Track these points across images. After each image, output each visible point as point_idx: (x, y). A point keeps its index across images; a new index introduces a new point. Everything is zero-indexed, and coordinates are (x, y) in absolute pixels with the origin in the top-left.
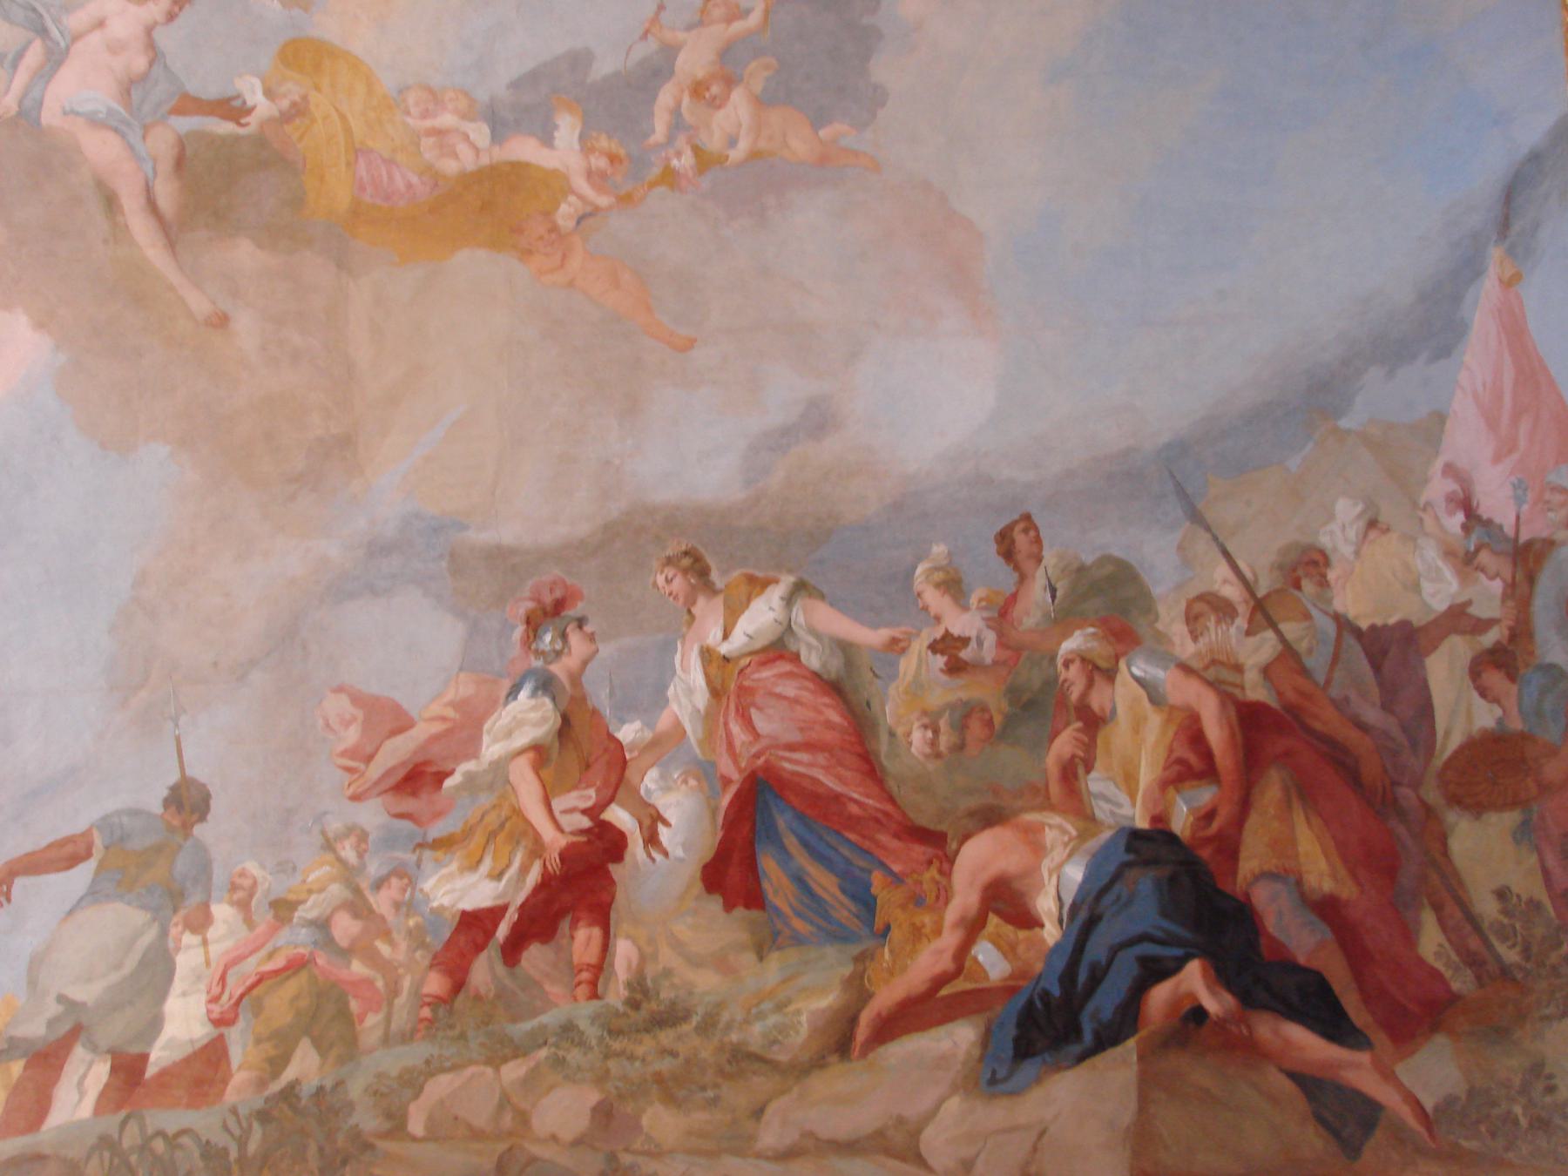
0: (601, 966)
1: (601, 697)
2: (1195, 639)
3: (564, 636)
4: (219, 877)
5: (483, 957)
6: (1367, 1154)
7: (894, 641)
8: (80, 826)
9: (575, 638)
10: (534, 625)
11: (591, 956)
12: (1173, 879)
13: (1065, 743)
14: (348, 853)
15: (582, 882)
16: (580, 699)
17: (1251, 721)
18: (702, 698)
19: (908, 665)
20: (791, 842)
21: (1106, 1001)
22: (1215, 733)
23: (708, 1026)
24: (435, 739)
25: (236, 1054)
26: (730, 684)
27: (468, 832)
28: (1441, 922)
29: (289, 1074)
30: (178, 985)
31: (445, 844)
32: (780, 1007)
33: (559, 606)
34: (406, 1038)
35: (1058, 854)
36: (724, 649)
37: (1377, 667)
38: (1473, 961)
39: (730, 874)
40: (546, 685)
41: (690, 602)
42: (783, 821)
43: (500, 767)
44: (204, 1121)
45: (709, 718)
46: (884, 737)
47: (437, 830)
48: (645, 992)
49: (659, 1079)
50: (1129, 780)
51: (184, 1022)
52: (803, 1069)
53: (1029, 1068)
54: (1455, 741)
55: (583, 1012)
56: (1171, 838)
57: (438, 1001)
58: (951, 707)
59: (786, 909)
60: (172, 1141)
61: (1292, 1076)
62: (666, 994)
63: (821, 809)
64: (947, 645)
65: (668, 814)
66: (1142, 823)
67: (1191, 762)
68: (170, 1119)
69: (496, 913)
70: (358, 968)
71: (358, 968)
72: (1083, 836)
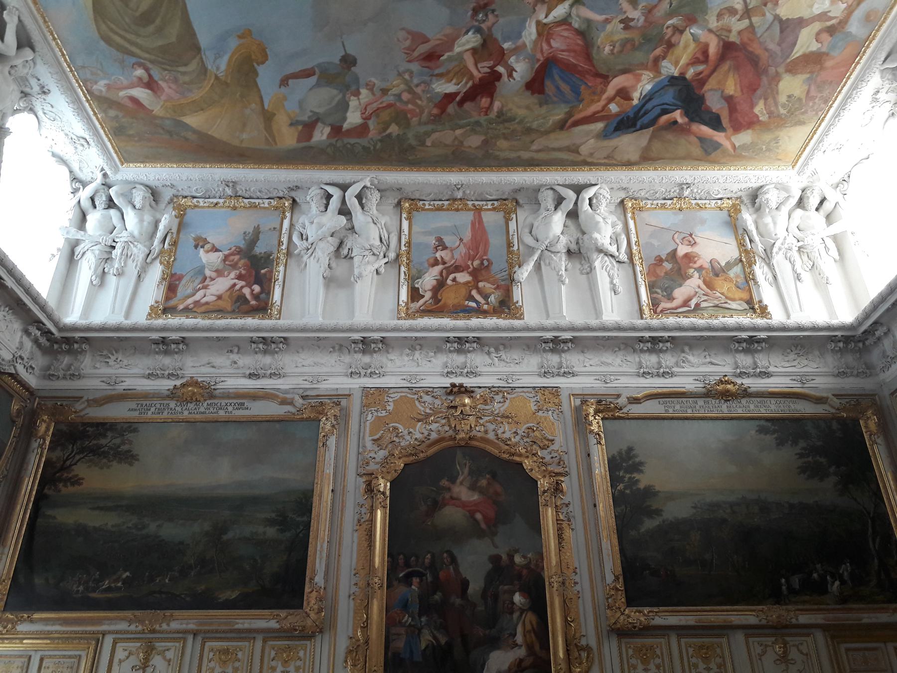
1: (498, 36)
2: (718, 20)
3: (487, 15)
4: (362, 82)
5: (451, 106)
6: (713, 155)
7: (607, 19)
9: (490, 16)
10: (476, 11)
11: (487, 105)
12: (680, 90)
13: (658, 51)
14: (407, 76)
16: (490, 35)
17: (728, 48)
18: (534, 36)
19: (609, 27)
20: (557, 77)
22: (713, 50)
23: (519, 123)
24: (438, 45)
25: (371, 127)
26: (545, 31)
27: (448, 72)
28: (765, 104)
29: (388, 131)
30: (351, 109)
31: (441, 75)
32: (544, 118)
33: (486, 5)
34: (425, 124)
35: (645, 82)
36: (545, 21)
37: (782, 31)
38: (770, 114)
39: (535, 85)
40: (478, 30)
41: (535, 5)
42: (555, 72)
43: (460, 54)
44: (364, 142)
45: (535, 42)
46: (596, 48)
47: (437, 72)
48: (503, 114)
49: (504, 134)
50: (676, 63)
51: (353, 118)
52: (547, 133)
53: (618, 133)
54: (797, 55)
55: (483, 119)
56: (685, 79)
57: (435, 116)
58: (622, 40)
59: (551, 94)
60: (353, 145)
61: (697, 137)
62: (509, 114)
63: (569, 69)
64: (626, 23)
65: (517, 69)
66: (676, 74)
67: (702, 55)
68: (352, 141)
69: (456, 94)
70: (410, 106)
71: (410, 106)
72: (654, 78)
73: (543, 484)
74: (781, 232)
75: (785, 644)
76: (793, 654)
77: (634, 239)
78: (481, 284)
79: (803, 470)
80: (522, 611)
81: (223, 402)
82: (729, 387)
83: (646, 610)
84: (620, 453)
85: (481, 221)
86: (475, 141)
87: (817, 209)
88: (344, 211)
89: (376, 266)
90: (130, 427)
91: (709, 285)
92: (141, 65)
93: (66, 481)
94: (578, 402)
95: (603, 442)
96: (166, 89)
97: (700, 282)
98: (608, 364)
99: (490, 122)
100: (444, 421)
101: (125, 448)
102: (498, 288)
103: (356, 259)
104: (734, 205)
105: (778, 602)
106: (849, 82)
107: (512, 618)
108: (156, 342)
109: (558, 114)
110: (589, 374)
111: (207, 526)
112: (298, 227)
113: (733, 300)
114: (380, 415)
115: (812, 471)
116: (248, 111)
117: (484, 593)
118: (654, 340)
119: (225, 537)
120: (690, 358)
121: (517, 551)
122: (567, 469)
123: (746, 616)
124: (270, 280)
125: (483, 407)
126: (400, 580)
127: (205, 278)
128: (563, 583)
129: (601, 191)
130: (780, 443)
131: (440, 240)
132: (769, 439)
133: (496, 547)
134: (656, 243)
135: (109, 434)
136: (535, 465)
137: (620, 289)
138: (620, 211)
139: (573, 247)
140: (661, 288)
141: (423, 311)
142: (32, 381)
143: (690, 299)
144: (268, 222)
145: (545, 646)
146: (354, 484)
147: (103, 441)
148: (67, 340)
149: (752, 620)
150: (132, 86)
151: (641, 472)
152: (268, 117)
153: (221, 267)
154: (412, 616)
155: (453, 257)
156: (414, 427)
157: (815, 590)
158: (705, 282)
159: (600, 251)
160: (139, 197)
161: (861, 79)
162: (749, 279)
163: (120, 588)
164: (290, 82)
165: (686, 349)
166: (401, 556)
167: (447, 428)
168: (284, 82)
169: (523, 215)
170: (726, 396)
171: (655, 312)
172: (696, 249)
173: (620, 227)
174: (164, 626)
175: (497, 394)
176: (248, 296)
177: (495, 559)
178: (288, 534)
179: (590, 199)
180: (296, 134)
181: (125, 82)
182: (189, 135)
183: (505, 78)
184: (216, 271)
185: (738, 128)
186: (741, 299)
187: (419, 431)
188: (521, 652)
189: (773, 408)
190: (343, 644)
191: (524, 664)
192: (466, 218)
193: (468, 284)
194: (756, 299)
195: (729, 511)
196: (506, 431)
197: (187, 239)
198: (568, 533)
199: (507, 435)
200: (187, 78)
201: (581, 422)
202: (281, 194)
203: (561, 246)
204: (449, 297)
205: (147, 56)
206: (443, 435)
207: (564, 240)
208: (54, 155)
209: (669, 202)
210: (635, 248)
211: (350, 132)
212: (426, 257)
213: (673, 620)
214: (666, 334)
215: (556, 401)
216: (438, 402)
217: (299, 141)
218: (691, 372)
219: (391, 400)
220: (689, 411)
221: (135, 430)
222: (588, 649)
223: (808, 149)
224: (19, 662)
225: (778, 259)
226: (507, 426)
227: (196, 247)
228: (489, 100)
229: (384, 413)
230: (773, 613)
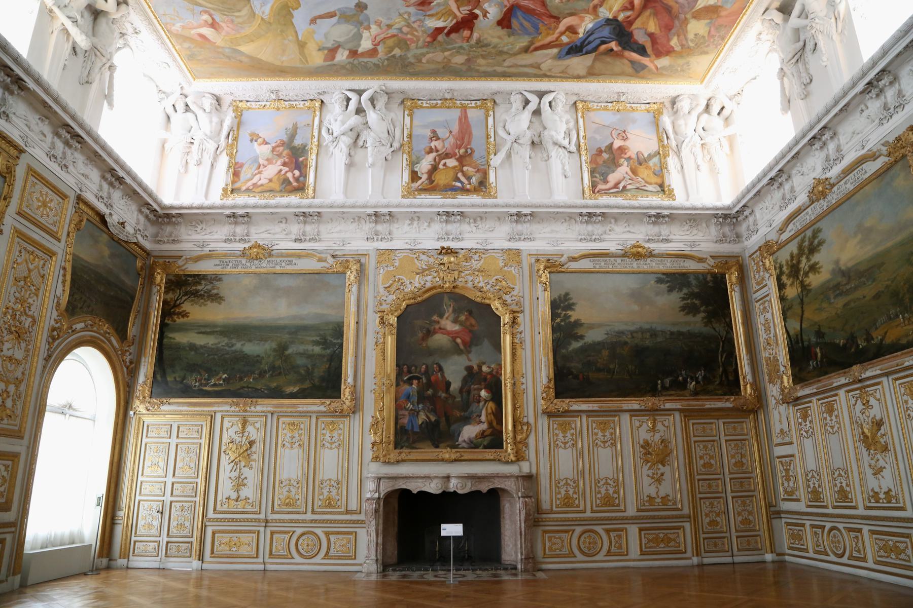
0: (468, 39)
4: (372, 20)
6: (641, 73)
8: (332, 10)
14: (406, 16)
15: (468, 23)
20: (521, 18)
21: (590, 47)
27: (437, 14)
31: (432, 15)
38: (682, 46)
39: (505, 22)
42: (519, 13)
44: (374, 60)
47: (428, 13)
50: (610, 10)
51: (366, 44)
52: (515, 54)
55: (465, 45)
56: (617, 20)
57: (429, 42)
62: (485, 42)
63: (528, 11)
66: (611, 17)
68: (366, 60)
69: (444, 28)
70: (409, 36)
73: (506, 318)
74: (690, 132)
75: (655, 420)
76: (659, 426)
77: (582, 134)
78: (465, 168)
79: (683, 309)
80: (486, 401)
81: (279, 259)
82: (640, 250)
83: (568, 400)
84: (560, 297)
85: (466, 117)
86: (459, 59)
87: (719, 114)
88: (360, 111)
89: (385, 155)
90: (217, 278)
91: (634, 172)
92: (206, 12)
93: (179, 314)
94: (533, 260)
95: (548, 289)
96: (226, 28)
97: (628, 170)
98: (557, 232)
99: (471, 46)
100: (435, 275)
101: (214, 292)
102: (478, 171)
103: (370, 149)
104: (658, 109)
105: (654, 396)
106: (739, 27)
108: (229, 217)
109: (523, 42)
110: (543, 239)
111: (274, 345)
112: (326, 123)
113: (650, 184)
115: (689, 309)
116: (286, 42)
117: (461, 391)
118: (590, 215)
119: (287, 353)
120: (615, 228)
121: (484, 363)
123: (634, 404)
124: (306, 166)
125: (464, 264)
126: (405, 382)
127: (259, 166)
128: (514, 384)
129: (559, 96)
130: (670, 290)
131: (434, 132)
132: (664, 286)
133: (470, 360)
134: (598, 137)
135: (203, 282)
137: (569, 174)
138: (573, 110)
139: (536, 140)
140: (599, 173)
141: (421, 190)
142: (148, 245)
143: (618, 183)
144: (302, 119)
145: (500, 422)
146: (373, 320)
147: (199, 288)
148: (168, 216)
149: (636, 406)
150: (200, 26)
151: (573, 310)
152: (302, 45)
153: (270, 156)
154: (412, 404)
155: (444, 146)
157: (679, 386)
158: (631, 170)
159: (555, 144)
160: (208, 103)
161: (747, 25)
162: (663, 167)
163: (221, 385)
164: (318, 21)
165: (613, 221)
168: (313, 21)
169: (499, 110)
170: (638, 256)
171: (594, 192)
172: (627, 143)
173: (572, 124)
174: (253, 408)
175: (476, 253)
176: (291, 179)
177: (469, 369)
178: (328, 351)
179: (550, 103)
180: (323, 57)
181: (195, 24)
182: (243, 58)
183: (481, 17)
184: (267, 160)
185: (659, 54)
186: (656, 184)
187: (418, 282)
188: (484, 426)
189: (669, 266)
190: (369, 421)
192: (455, 114)
193: (453, 167)
194: (667, 183)
195: (630, 336)
196: (481, 281)
197: (244, 135)
198: (519, 352)
199: (480, 285)
200: (240, 20)
201: (533, 274)
202: (312, 98)
203: (526, 141)
204: (441, 178)
205: (210, 6)
207: (529, 134)
208: (144, 75)
209: (610, 105)
210: (582, 141)
211: (363, 54)
212: (423, 146)
213: (584, 407)
214: (598, 211)
216: (432, 260)
217: (325, 60)
218: (615, 238)
220: (611, 267)
221: (220, 280)
222: (528, 424)
223: (711, 71)
224: (165, 428)
225: (685, 152)
227: (251, 141)
228: (469, 32)
230: (649, 402)
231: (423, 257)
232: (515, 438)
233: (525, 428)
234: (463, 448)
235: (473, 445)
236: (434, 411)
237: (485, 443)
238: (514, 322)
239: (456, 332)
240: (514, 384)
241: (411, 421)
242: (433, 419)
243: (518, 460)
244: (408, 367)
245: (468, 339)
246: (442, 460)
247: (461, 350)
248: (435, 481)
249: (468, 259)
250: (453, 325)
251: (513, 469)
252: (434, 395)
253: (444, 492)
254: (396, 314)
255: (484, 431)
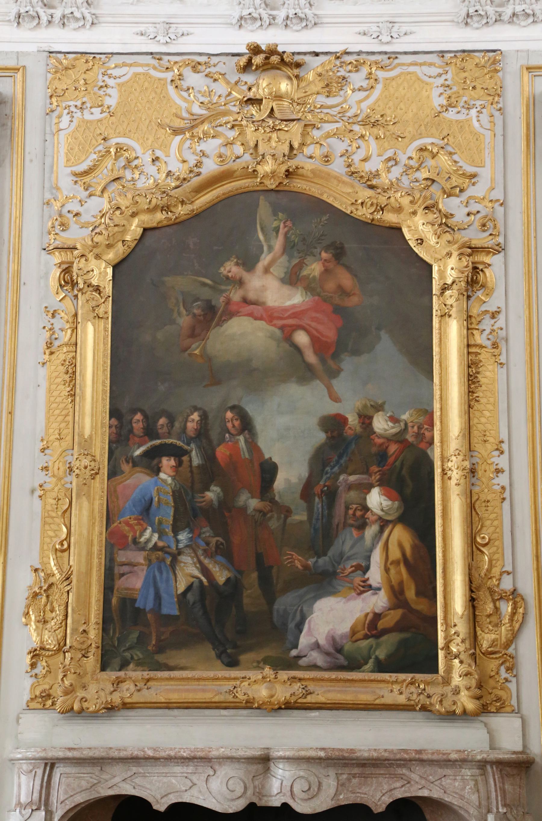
73: (448, 270)
80: (383, 524)
100: (232, 134)
107: (362, 538)
114: (87, 116)
117: (307, 492)
121: (379, 408)
122: (501, 239)
125: (321, 100)
126: (135, 463)
128: (473, 471)
133: (336, 399)
136: (428, 233)
145: (427, 589)
156: (165, 147)
166: (138, 416)
167: (239, 150)
175: (357, 67)
177: (333, 425)
188: (379, 601)
191: (381, 625)
196: (372, 156)
198: (489, 373)
206: (230, 165)
215: (489, 83)
216: (221, 88)
219: (111, 82)
222: (514, 595)
226: (373, 143)
229: (97, 114)
231: (193, 79)
232: (474, 638)
233: (506, 608)
234: (314, 667)
235: (343, 658)
236: (224, 552)
237: (381, 654)
238: (474, 280)
239: (297, 313)
240: (473, 471)
241: (152, 582)
242: (221, 576)
243: (484, 710)
244: (146, 417)
245: (329, 333)
246: (249, 705)
247: (309, 367)
248: (225, 771)
249: (332, 85)
250: (286, 290)
251: (467, 739)
252: (226, 504)
253: (252, 806)
254: (111, 256)
255: (377, 617)
